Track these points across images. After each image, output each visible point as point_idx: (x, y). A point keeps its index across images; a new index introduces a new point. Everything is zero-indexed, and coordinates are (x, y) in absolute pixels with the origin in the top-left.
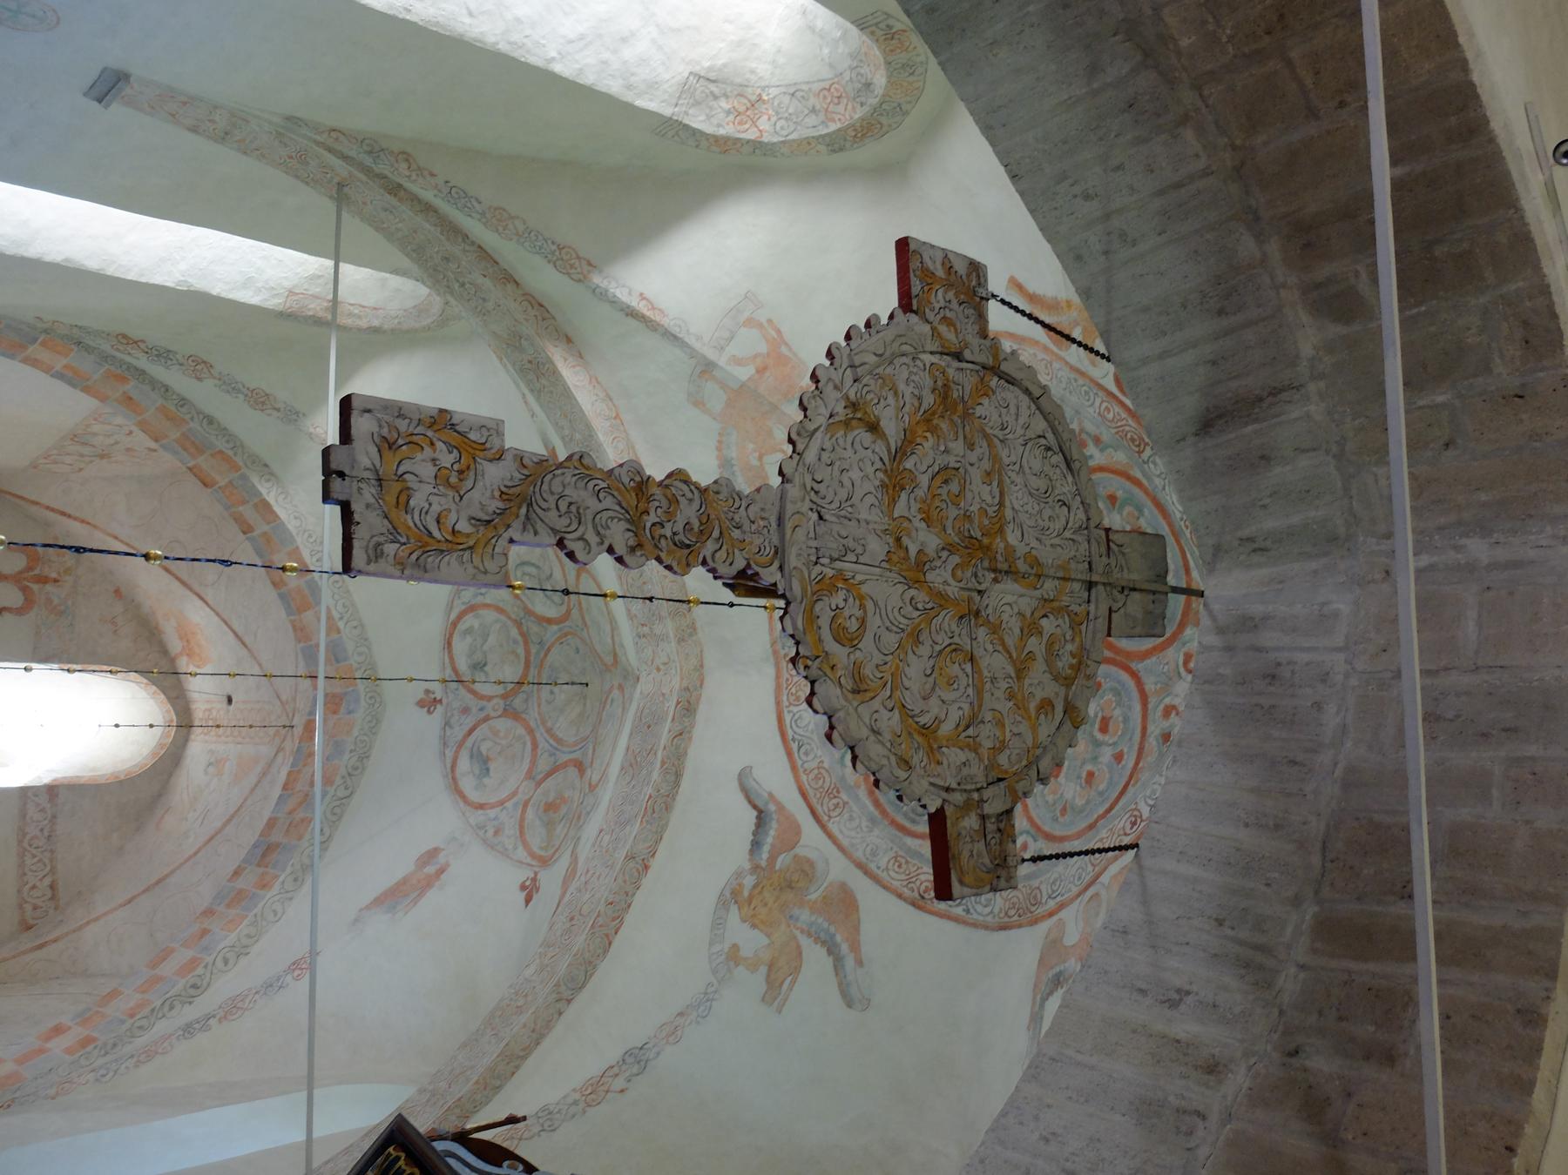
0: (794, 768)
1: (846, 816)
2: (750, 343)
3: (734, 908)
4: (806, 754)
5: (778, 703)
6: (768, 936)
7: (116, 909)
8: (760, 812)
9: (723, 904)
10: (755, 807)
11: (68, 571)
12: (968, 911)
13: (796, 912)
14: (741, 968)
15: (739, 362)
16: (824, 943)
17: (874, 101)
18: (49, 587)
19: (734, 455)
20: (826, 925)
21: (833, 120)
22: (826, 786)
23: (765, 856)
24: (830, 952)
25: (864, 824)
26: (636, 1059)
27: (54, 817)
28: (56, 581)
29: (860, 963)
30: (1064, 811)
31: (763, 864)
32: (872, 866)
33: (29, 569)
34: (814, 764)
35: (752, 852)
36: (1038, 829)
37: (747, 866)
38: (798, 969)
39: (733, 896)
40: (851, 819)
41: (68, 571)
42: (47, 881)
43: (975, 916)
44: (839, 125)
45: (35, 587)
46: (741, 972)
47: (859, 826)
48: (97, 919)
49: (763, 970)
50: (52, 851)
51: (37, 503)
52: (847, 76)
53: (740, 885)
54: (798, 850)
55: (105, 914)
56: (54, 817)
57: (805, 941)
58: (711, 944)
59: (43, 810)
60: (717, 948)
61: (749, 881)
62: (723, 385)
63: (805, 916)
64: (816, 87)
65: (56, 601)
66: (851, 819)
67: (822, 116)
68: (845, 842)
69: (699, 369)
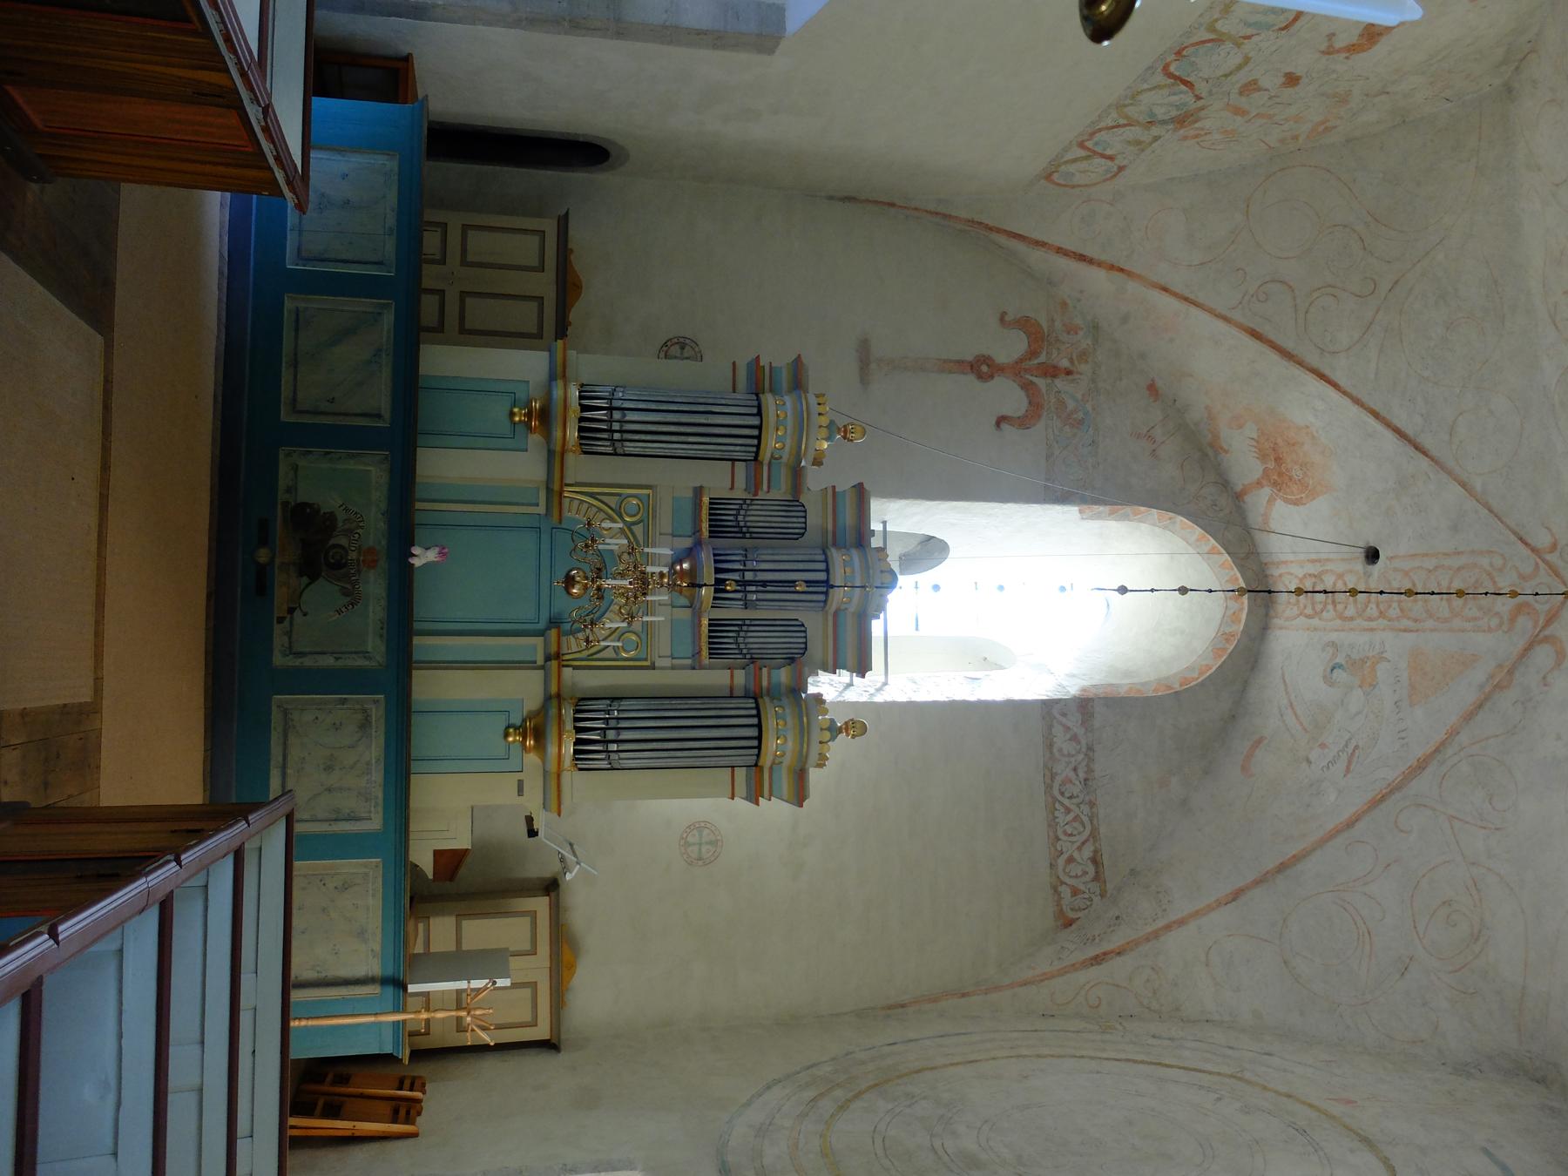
7: (1210, 909)
11: (1083, 356)
18: (1059, 383)
27: (1090, 748)
28: (1069, 373)
33: (1033, 354)
41: (1083, 356)
42: (1087, 852)
45: (1041, 382)
48: (1181, 922)
50: (1092, 804)
51: (1043, 244)
55: (1196, 914)
56: (1090, 748)
59: (1074, 738)
65: (1071, 405)
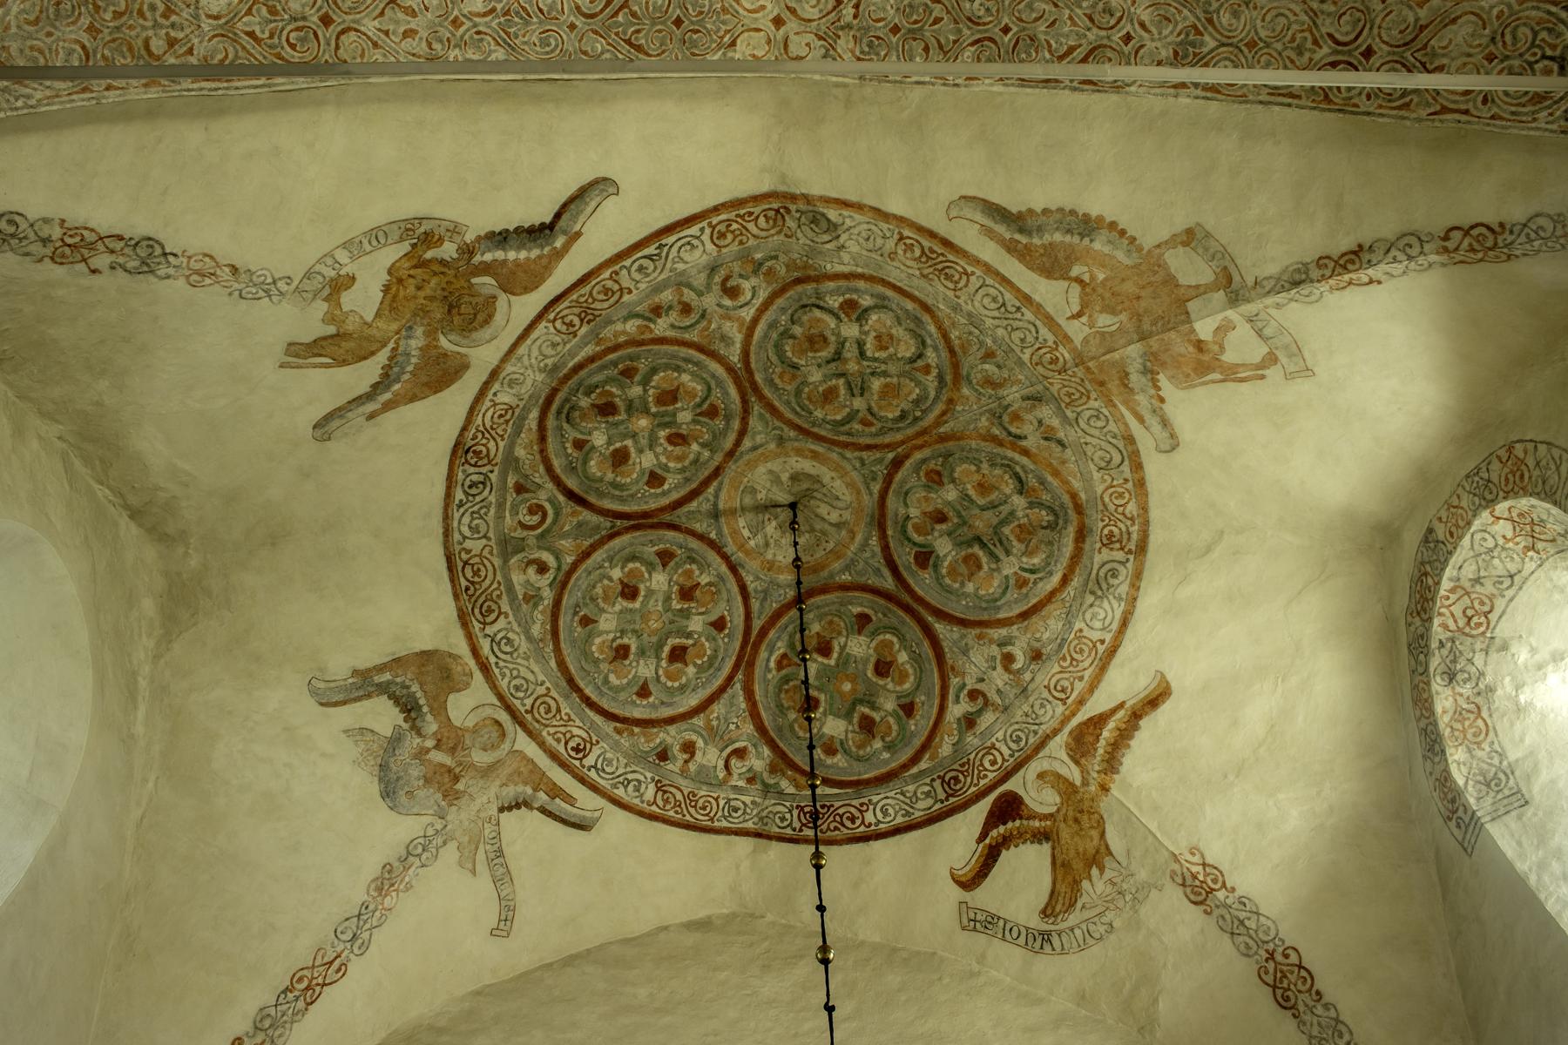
0: (620, 256)
1: (558, 339)
2: (1242, 346)
3: (406, 247)
4: (641, 269)
5: (716, 209)
6: (378, 315)
8: (551, 227)
9: (408, 227)
10: (558, 216)
12: (461, 505)
13: (419, 331)
14: (325, 306)
15: (1224, 329)
16: (386, 375)
17: (1435, 662)
19: (1097, 246)
20: (410, 368)
21: (1452, 591)
22: (597, 305)
23: (488, 257)
24: (375, 386)
25: (549, 362)
26: (146, 255)
29: (371, 416)
30: (586, 621)
31: (477, 259)
32: (497, 386)
34: (626, 283)
35: (491, 236)
36: (564, 585)
37: (469, 237)
38: (344, 363)
39: (422, 236)
40: (554, 345)
43: (457, 515)
44: (1442, 592)
46: (321, 307)
47: (546, 357)
49: (332, 330)
52: (1479, 660)
53: (441, 240)
54: (503, 298)
57: (382, 357)
58: (344, 245)
60: (342, 256)
61: (448, 250)
62: (1199, 291)
63: (416, 343)
64: (1500, 604)
66: (554, 345)
67: (1467, 585)
68: (522, 350)
69: (1236, 278)
